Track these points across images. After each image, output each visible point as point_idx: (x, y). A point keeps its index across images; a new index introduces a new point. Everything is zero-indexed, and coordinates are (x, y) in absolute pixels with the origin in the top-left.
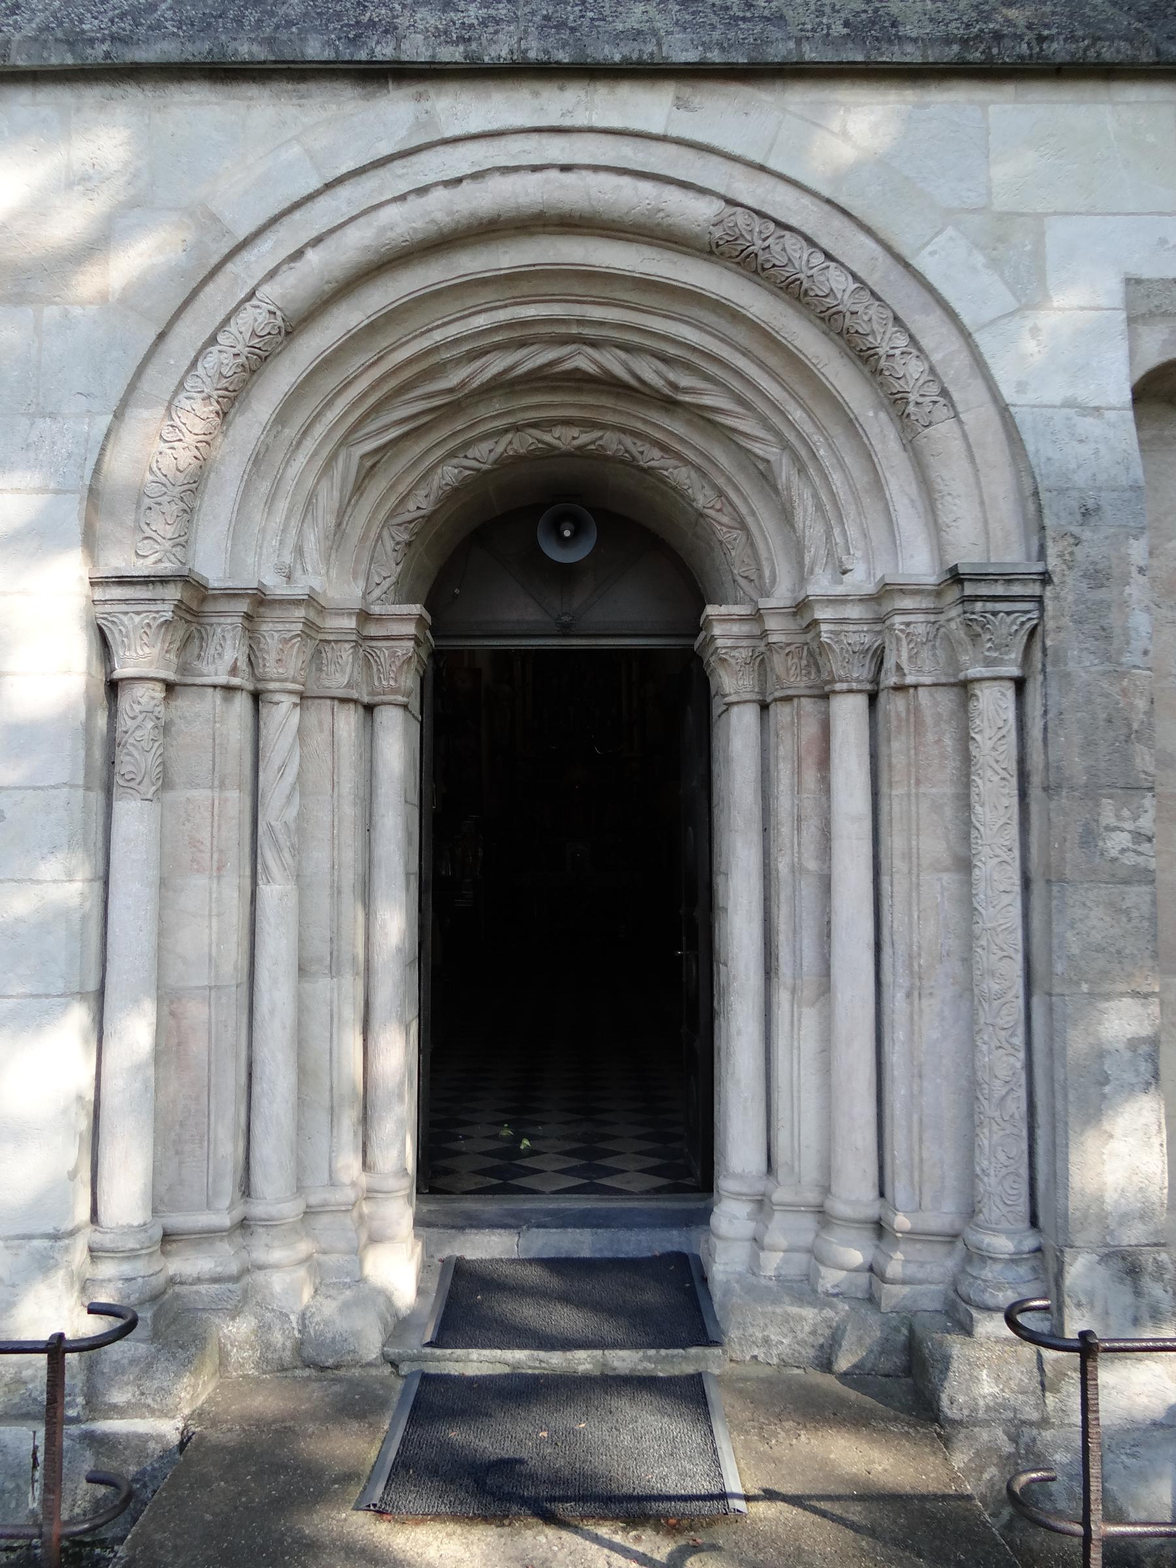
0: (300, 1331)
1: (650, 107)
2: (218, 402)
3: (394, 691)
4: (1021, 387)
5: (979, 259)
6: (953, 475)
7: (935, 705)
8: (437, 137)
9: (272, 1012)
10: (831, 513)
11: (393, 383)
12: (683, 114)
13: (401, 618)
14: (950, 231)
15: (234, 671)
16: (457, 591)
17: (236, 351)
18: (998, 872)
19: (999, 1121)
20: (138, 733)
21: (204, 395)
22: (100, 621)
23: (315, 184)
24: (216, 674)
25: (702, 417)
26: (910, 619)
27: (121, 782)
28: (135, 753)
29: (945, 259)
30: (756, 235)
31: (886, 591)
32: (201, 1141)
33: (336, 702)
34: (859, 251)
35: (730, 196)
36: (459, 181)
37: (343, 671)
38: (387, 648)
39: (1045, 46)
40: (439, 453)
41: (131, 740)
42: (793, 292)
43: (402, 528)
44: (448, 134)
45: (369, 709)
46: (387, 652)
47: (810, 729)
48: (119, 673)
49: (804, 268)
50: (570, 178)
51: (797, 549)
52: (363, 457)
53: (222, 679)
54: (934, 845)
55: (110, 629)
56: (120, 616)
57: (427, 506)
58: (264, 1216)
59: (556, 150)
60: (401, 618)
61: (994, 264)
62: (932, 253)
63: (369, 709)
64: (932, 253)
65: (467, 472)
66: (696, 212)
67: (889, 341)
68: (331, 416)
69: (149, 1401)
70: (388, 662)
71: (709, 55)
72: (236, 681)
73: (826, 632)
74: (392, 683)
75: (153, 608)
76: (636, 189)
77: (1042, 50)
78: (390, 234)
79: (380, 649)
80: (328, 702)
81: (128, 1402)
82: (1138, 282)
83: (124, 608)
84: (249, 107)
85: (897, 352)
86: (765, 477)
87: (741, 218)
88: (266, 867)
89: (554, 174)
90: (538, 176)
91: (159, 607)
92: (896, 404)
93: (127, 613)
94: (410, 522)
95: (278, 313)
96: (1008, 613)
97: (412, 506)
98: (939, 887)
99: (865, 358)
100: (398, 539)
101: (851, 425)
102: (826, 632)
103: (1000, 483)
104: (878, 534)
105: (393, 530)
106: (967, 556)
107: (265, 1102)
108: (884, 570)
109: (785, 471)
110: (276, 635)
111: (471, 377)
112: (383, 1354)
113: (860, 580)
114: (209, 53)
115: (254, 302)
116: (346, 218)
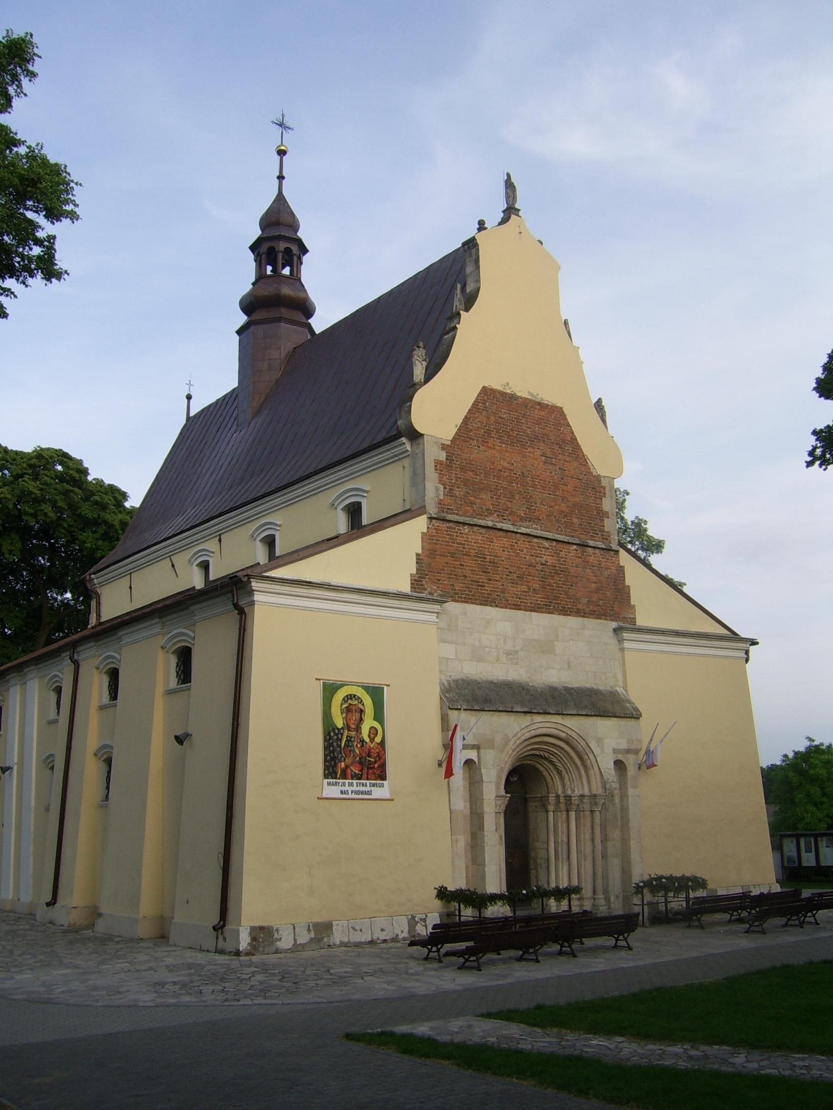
6: (593, 779)
7: (588, 813)
10: (572, 781)
18: (598, 841)
25: (551, 762)
26: (586, 800)
29: (593, 745)
31: (582, 796)
34: (583, 743)
42: (573, 748)
47: (564, 816)
51: (564, 785)
54: (588, 836)
59: (547, 725)
66: (563, 735)
67: (586, 757)
86: (560, 773)
92: (585, 766)
98: (589, 844)
99: (581, 758)
101: (578, 768)
103: (599, 779)
104: (580, 785)
106: (595, 792)
108: (581, 792)
109: (564, 772)
113: (577, 793)
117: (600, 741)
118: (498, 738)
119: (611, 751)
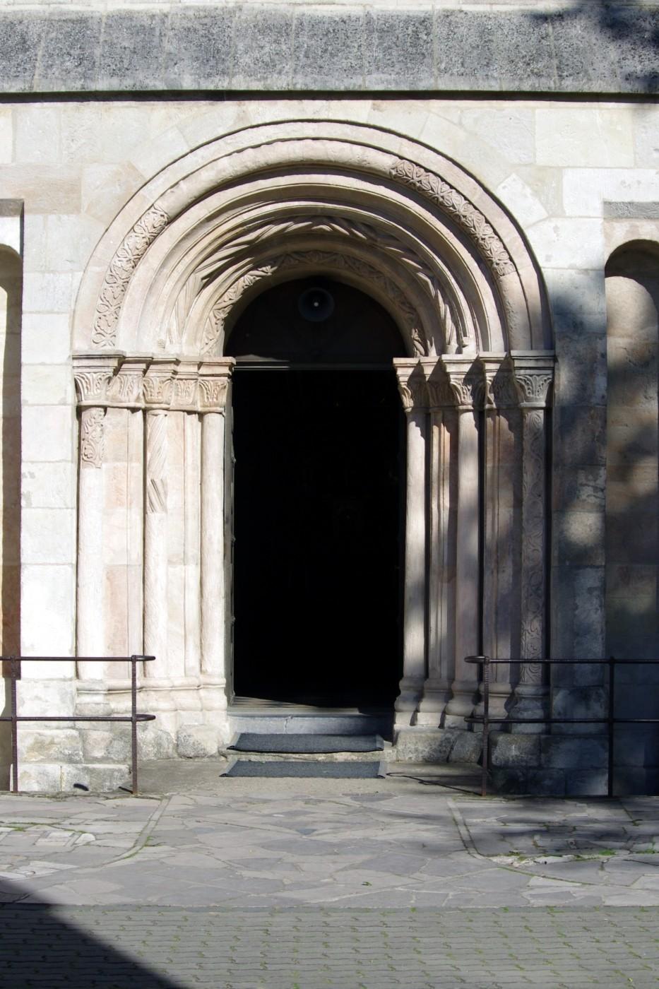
0: (176, 740)
1: (360, 110)
2: (134, 262)
3: (216, 405)
4: (548, 258)
5: (528, 191)
8: (249, 125)
9: (156, 580)
11: (220, 241)
12: (376, 113)
13: (220, 364)
14: (514, 176)
15: (138, 399)
16: (248, 335)
17: (143, 236)
19: (530, 631)
20: (94, 433)
21: (127, 259)
22: (76, 377)
23: (188, 151)
24: (129, 401)
27: (85, 458)
28: (92, 444)
30: (415, 174)
32: (124, 643)
33: (186, 413)
35: (401, 154)
36: (259, 146)
37: (189, 395)
38: (212, 381)
39: (563, 83)
40: (245, 269)
41: (90, 437)
43: (220, 311)
44: (254, 123)
45: (201, 416)
46: (212, 383)
48: (84, 403)
49: (439, 192)
50: (318, 143)
52: (203, 279)
53: (132, 404)
55: (80, 381)
56: (87, 374)
57: (236, 298)
58: (155, 685)
59: (310, 130)
60: (220, 364)
61: (536, 193)
62: (504, 188)
63: (201, 416)
64: (504, 188)
65: (258, 278)
68: (188, 259)
69: (112, 756)
70: (213, 388)
71: (389, 86)
72: (138, 405)
73: (454, 379)
74: (215, 400)
75: (103, 370)
76: (351, 150)
77: (561, 84)
78: (224, 174)
79: (208, 381)
80: (182, 413)
81: (103, 757)
82: (610, 203)
83: (88, 370)
84: (152, 109)
85: (486, 237)
87: (406, 166)
88: (151, 503)
89: (310, 141)
90: (301, 142)
91: (106, 370)
93: (89, 373)
94: (225, 308)
95: (166, 215)
96: (538, 375)
97: (226, 298)
100: (218, 317)
102: (454, 379)
105: (216, 312)
107: (153, 627)
110: (158, 379)
111: (262, 234)
112: (219, 751)
114: (134, 86)
115: (152, 209)
116: (201, 166)
117: (544, 180)
118: (98, 182)
119: (597, 209)
